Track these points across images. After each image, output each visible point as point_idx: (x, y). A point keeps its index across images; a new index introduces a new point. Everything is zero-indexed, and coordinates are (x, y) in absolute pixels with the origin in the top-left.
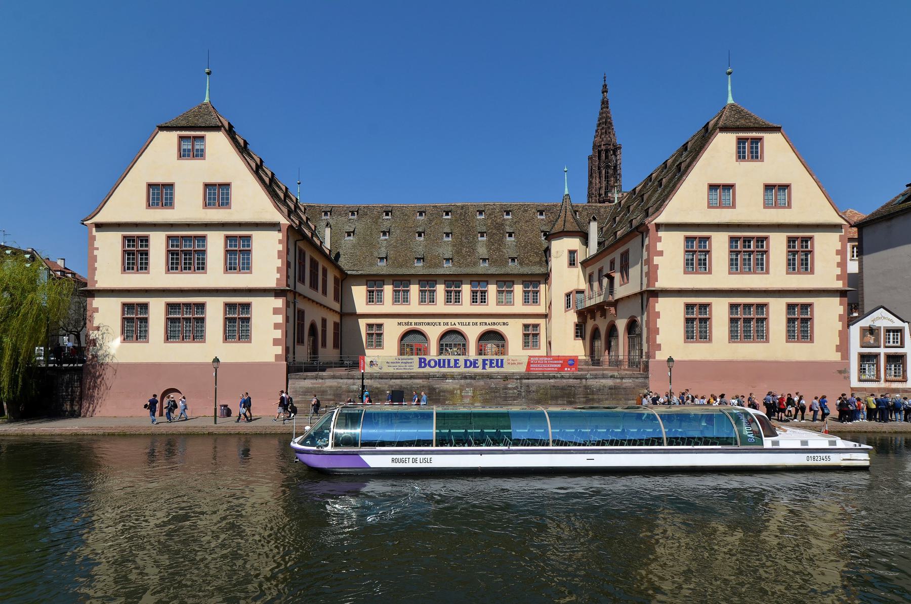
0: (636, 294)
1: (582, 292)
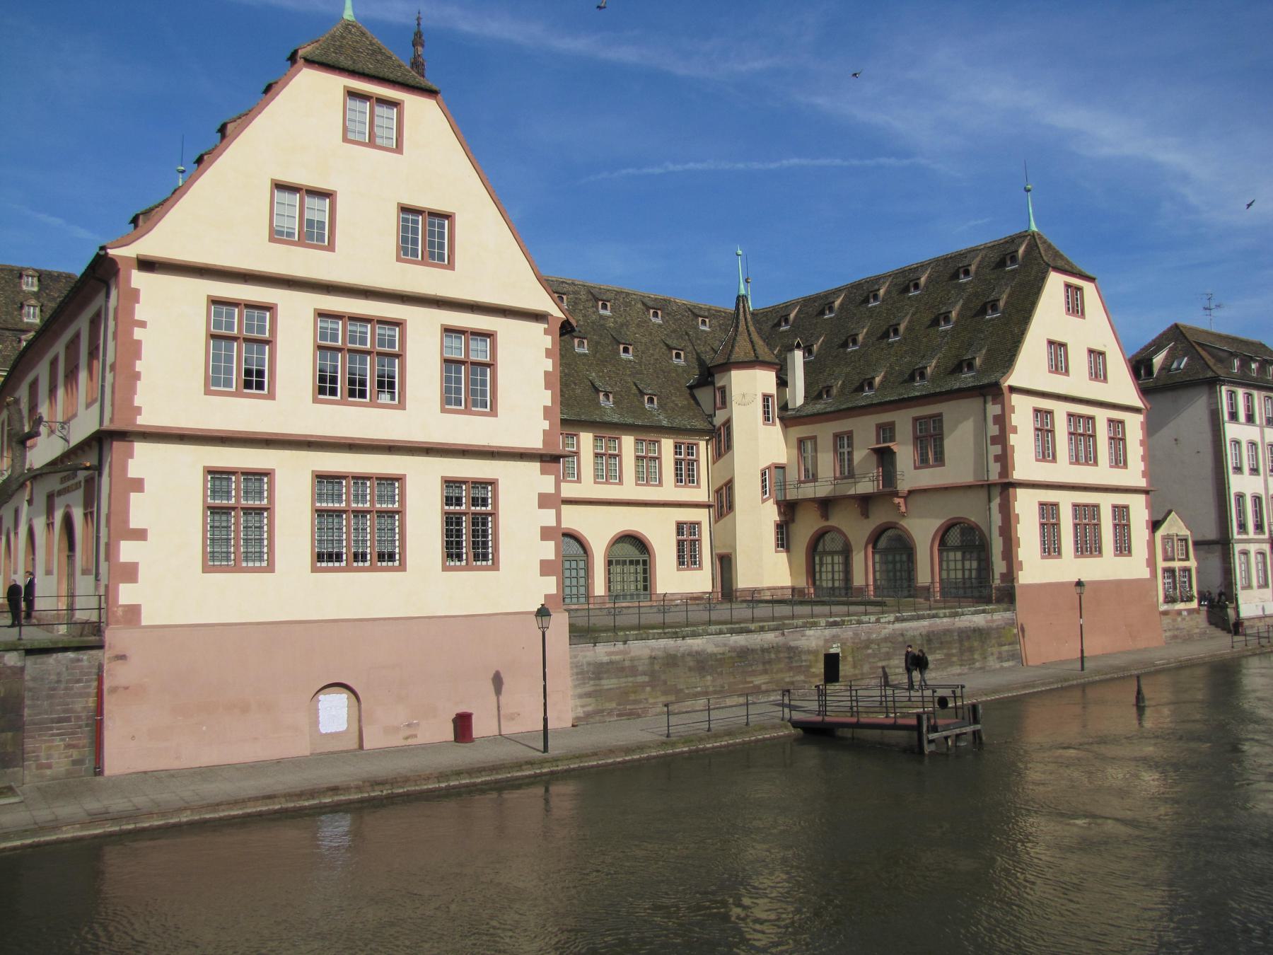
0: (982, 486)
1: (781, 467)
